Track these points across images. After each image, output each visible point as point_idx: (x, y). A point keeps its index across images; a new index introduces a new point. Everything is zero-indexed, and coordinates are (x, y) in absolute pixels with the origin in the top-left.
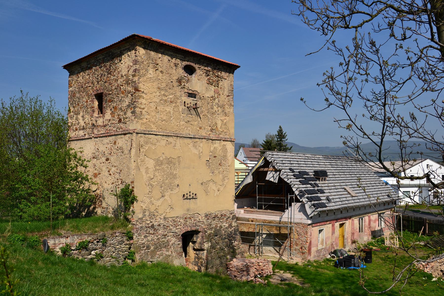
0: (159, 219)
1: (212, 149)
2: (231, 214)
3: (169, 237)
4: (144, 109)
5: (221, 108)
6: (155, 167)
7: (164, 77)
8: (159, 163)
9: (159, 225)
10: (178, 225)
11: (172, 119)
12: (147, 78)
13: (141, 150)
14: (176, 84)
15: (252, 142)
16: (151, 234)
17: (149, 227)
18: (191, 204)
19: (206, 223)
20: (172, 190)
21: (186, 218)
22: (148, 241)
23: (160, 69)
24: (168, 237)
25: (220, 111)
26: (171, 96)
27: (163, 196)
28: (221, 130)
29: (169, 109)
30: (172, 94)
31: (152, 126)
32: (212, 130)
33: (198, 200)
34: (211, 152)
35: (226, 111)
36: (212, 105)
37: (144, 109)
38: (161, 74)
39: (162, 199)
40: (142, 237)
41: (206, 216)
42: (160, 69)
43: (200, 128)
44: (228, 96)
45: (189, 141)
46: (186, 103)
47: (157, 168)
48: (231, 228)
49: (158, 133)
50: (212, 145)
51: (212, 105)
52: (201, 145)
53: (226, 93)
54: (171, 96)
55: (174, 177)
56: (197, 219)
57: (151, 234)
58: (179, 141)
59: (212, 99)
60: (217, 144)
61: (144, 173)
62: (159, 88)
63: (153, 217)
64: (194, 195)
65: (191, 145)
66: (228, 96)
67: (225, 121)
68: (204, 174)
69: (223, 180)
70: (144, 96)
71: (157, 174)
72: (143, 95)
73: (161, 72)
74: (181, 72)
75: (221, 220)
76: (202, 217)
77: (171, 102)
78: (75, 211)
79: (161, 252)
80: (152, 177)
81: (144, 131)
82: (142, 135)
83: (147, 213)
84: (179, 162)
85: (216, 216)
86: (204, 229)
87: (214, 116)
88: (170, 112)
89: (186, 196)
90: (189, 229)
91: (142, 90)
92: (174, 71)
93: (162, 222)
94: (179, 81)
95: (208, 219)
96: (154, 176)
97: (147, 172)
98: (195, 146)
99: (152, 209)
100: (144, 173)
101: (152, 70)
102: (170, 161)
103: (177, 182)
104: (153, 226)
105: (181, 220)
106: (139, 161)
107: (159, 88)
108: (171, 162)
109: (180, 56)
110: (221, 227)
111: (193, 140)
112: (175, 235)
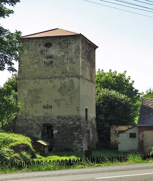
0: (30, 117)
1: (63, 82)
2: (77, 117)
3: (34, 125)
4: (22, 68)
5: (70, 60)
6: (28, 93)
7: (33, 52)
8: (30, 91)
9: (30, 119)
10: (40, 120)
11: (37, 71)
12: (24, 55)
13: (21, 86)
14: (39, 54)
15: (8, 80)
16: (25, 122)
17: (24, 119)
18: (49, 111)
19: (57, 121)
20: (37, 104)
21: (45, 117)
22: (23, 125)
23: (30, 49)
24: (33, 124)
25: (69, 62)
26: (36, 60)
27: (32, 106)
28: (69, 72)
29: (36, 66)
30: (37, 59)
31: (27, 75)
32: (63, 73)
33: (53, 109)
34: (62, 84)
35: (74, 61)
36: (63, 60)
37: (22, 68)
38: (31, 51)
39: (31, 108)
40: (20, 123)
41: (58, 117)
42: (30, 49)
43: (55, 73)
44: (75, 52)
45: (47, 80)
46: (46, 62)
47: (29, 93)
48: (74, 125)
49: (29, 78)
50: (63, 81)
51: (63, 60)
52: (55, 81)
53: (73, 51)
54: (36, 60)
55: (39, 97)
56: (52, 118)
57: (25, 122)
58: (42, 81)
59: (63, 56)
60: (66, 80)
61: (22, 96)
62: (30, 58)
63: (27, 115)
64: (50, 107)
65: (49, 82)
66: (75, 52)
67: (72, 67)
68: (58, 96)
69: (71, 98)
70: (22, 63)
71: (29, 96)
72: (22, 63)
73: (32, 50)
74: (43, 47)
75: (68, 120)
76: (55, 118)
77: (37, 63)
78: (6, 112)
79: (28, 131)
80: (26, 98)
81: (22, 78)
82: (21, 80)
83: (24, 114)
84: (41, 90)
85: (65, 118)
86: (55, 123)
87: (65, 65)
88: (36, 68)
89: (45, 107)
90: (46, 122)
91: (21, 61)
92: (39, 48)
93: (31, 118)
94: (42, 52)
95: (59, 119)
96: (27, 97)
97: (24, 96)
98: (51, 82)
99: (26, 111)
100: (22, 96)
101: (26, 51)
102: (36, 90)
103: (40, 100)
104: (26, 119)
105: (42, 118)
106: (20, 91)
107: (30, 58)
108: (37, 91)
109: (41, 40)
110: (67, 124)
111: (49, 79)
112: (37, 125)
